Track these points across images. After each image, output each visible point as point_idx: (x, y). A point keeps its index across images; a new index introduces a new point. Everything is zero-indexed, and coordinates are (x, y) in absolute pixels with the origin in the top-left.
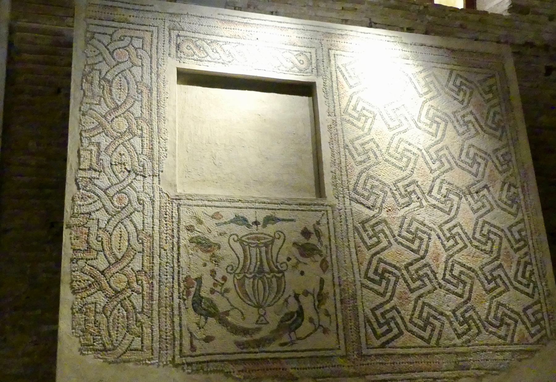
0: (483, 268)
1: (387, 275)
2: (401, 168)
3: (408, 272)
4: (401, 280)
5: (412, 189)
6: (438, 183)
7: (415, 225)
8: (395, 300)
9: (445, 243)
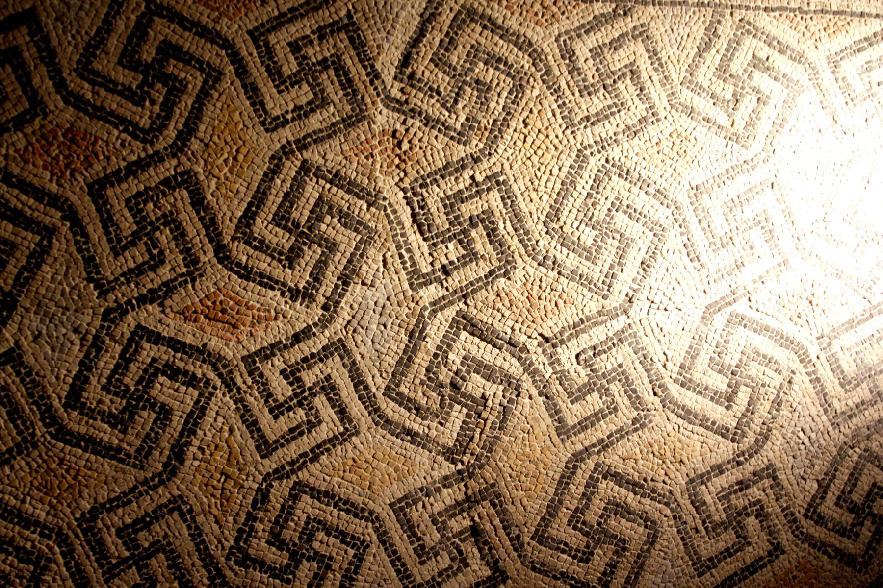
0: (182, 515)
1: (159, 93)
2: (555, 214)
3: (166, 182)
5: (478, 247)
6: (506, 366)
7: (346, 240)
9: (278, 362)
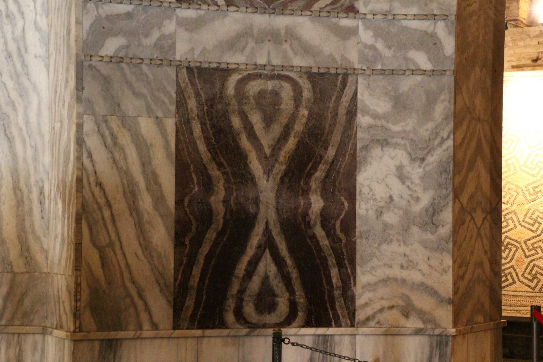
1: (509, 246)
4: (520, 250)
7: (537, 213)
8: (513, 263)
